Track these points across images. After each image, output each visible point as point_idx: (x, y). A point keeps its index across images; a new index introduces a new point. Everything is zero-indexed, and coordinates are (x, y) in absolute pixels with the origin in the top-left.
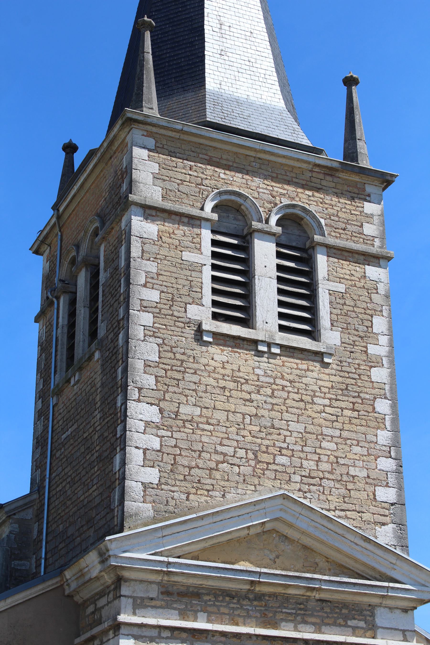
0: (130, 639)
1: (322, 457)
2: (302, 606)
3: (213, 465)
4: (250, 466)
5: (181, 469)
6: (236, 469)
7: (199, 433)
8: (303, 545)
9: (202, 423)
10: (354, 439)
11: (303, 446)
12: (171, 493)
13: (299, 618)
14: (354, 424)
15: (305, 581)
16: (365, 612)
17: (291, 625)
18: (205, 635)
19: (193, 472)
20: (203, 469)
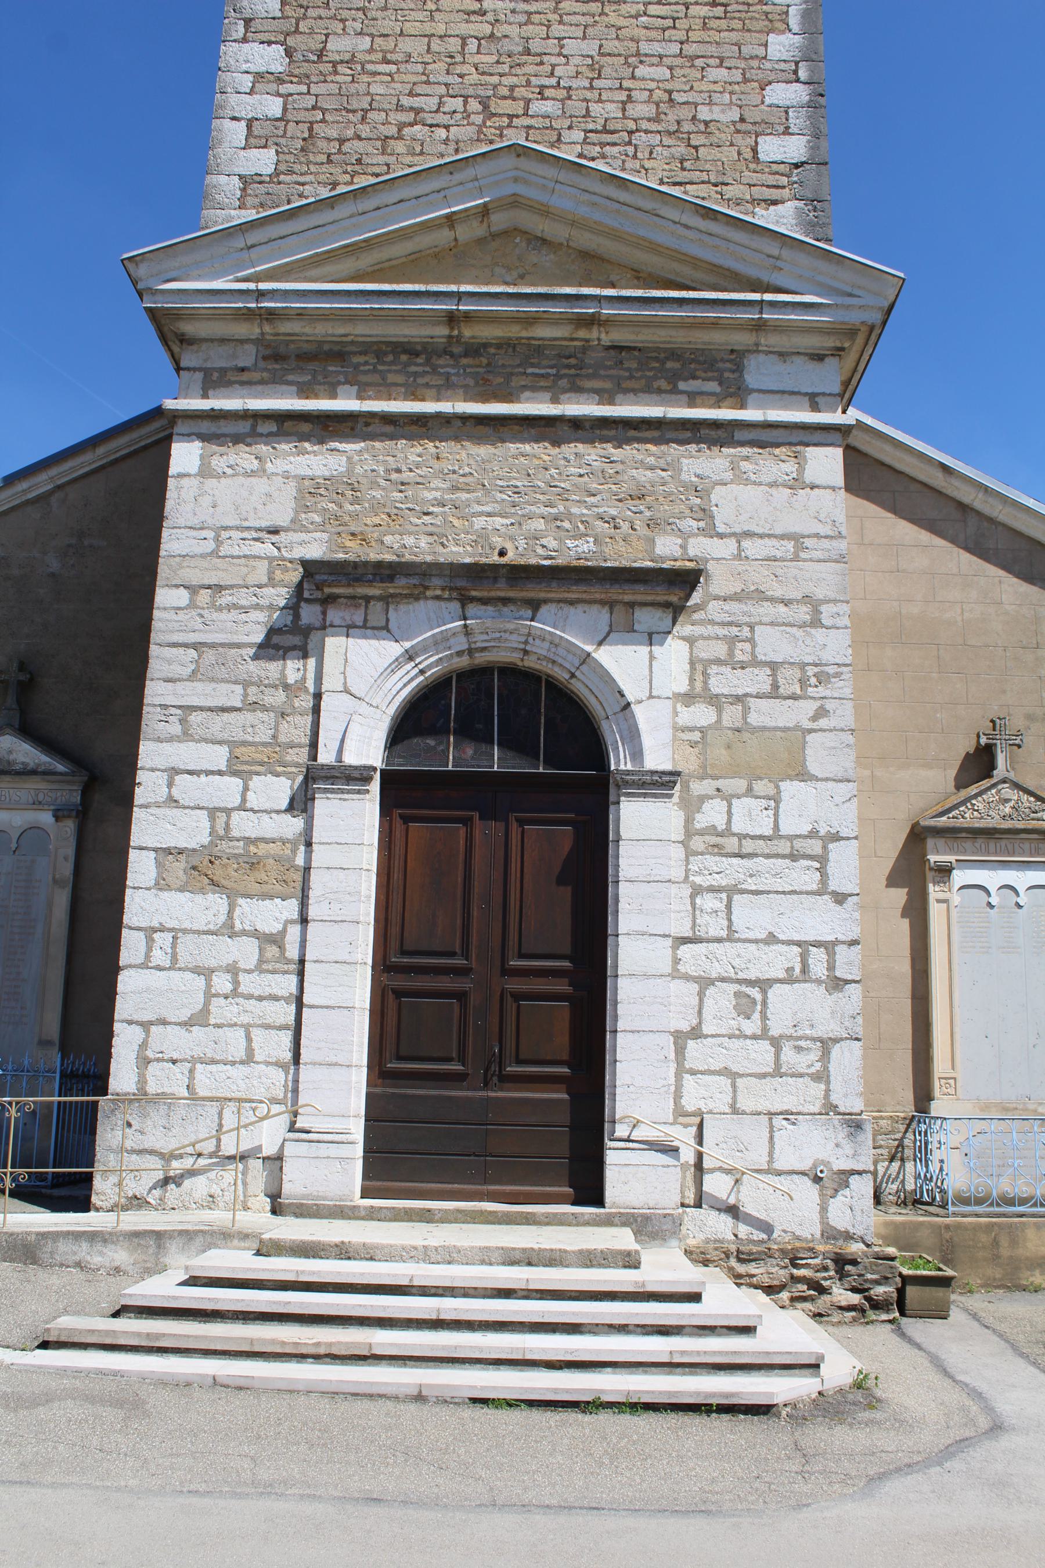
0: (193, 441)
1: (633, 93)
2: (573, 361)
3: (393, 131)
4: (473, 124)
5: (322, 144)
6: (442, 133)
7: (366, 80)
8: (580, 252)
9: (373, 62)
10: (712, 56)
11: (592, 79)
12: (297, 187)
13: (563, 383)
14: (712, 29)
15: (565, 304)
16: (721, 365)
17: (548, 395)
18: (350, 424)
19: (347, 147)
20: (370, 139)
